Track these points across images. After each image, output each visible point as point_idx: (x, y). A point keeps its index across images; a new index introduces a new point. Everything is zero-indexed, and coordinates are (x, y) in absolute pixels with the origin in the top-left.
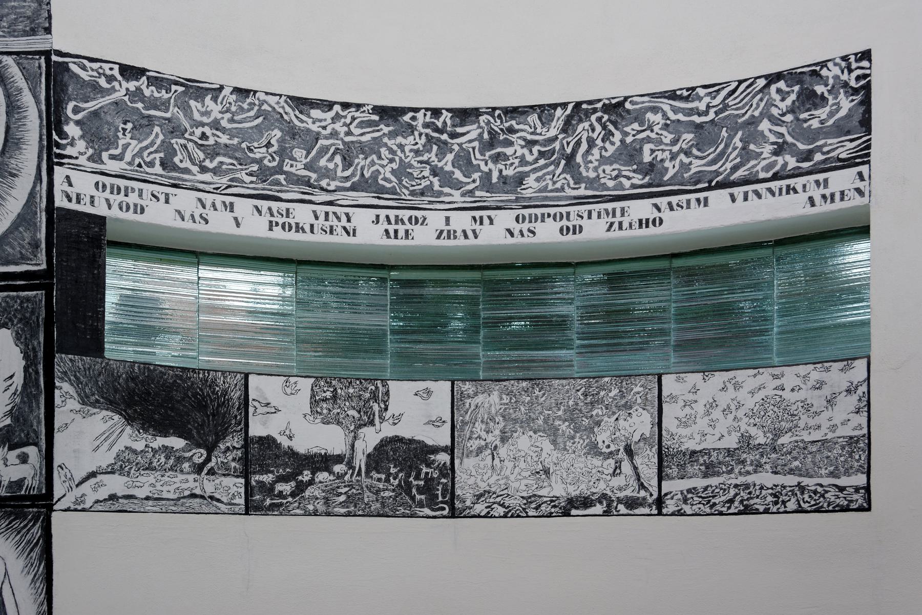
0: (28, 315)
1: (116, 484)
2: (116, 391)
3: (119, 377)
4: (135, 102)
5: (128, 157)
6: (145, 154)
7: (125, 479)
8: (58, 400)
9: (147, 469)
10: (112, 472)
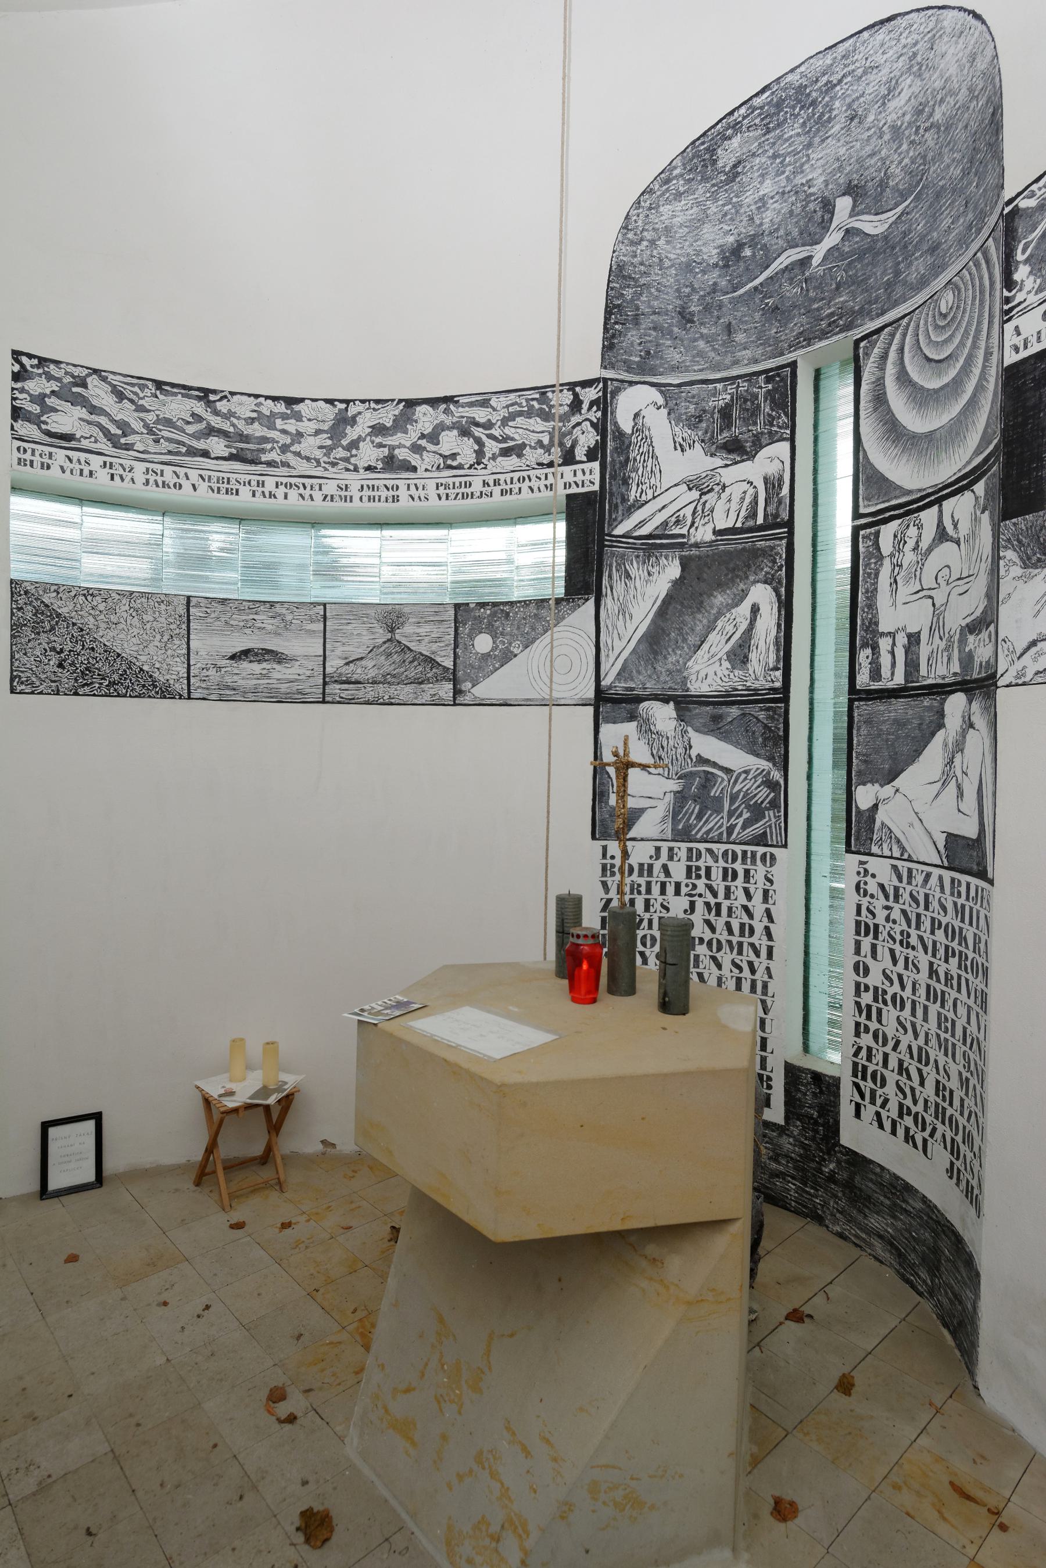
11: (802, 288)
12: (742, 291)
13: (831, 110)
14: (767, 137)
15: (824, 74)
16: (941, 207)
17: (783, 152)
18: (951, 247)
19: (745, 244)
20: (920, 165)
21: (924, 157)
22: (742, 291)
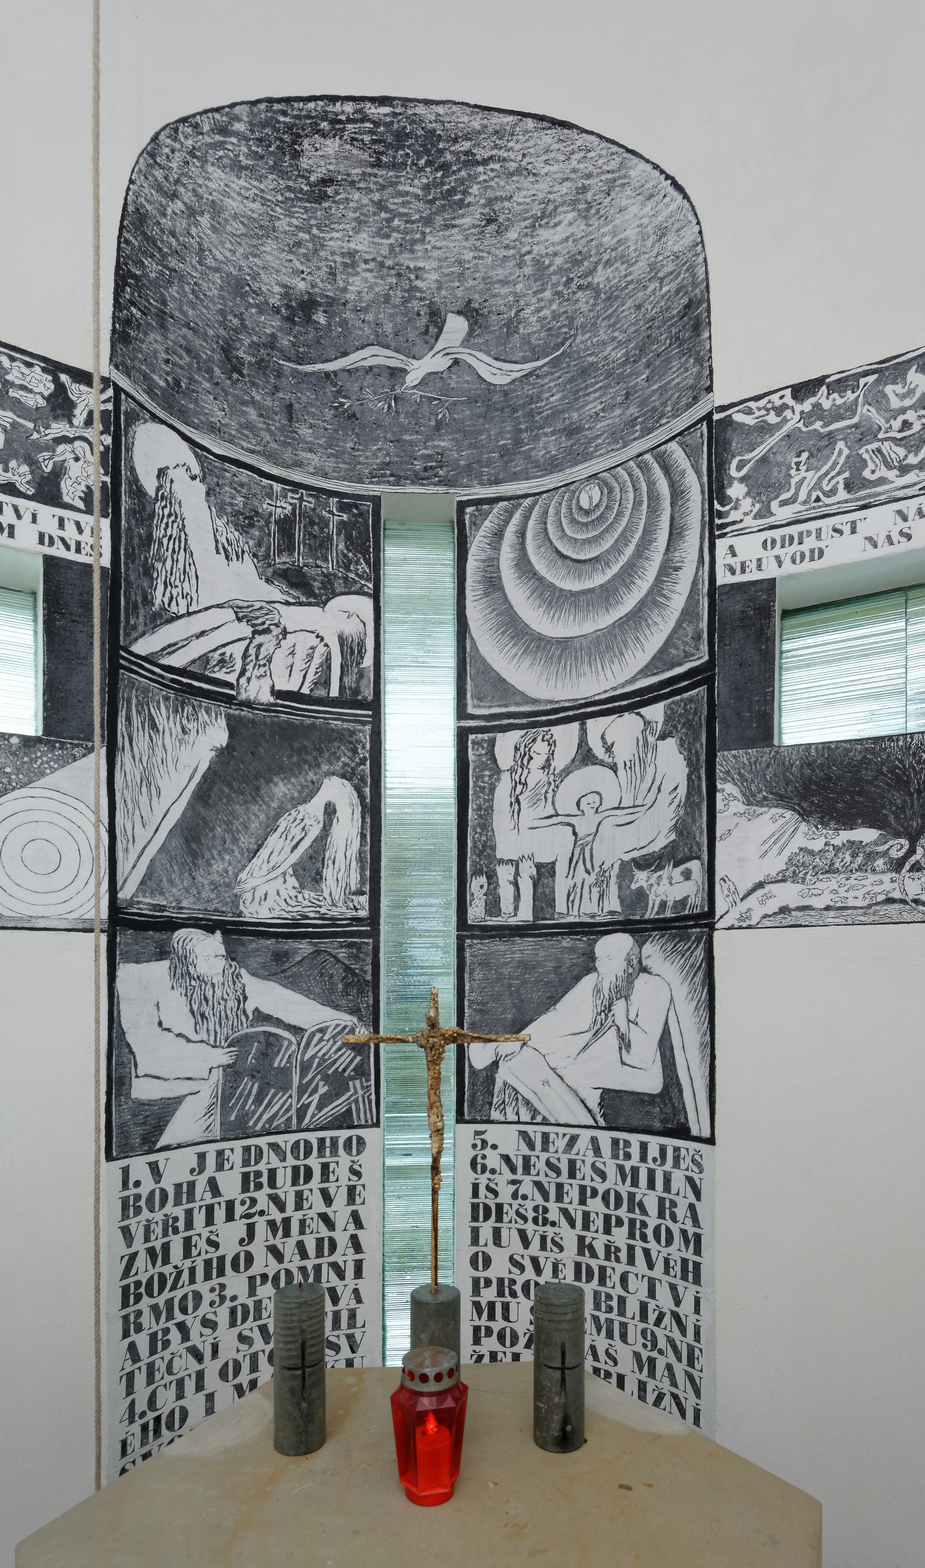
0: (690, 717)
1: (788, 894)
2: (788, 783)
3: (792, 765)
4: (812, 423)
5: (802, 496)
6: (825, 482)
7: (799, 887)
8: (719, 805)
9: (827, 872)
10: (784, 880)
11: (390, 406)
12: (309, 368)
13: (465, 193)
14: (375, 171)
15: (467, 138)
16: (587, 387)
17: (393, 207)
18: (597, 437)
19: (320, 305)
20: (564, 326)
21: (572, 319)
22: (309, 368)
